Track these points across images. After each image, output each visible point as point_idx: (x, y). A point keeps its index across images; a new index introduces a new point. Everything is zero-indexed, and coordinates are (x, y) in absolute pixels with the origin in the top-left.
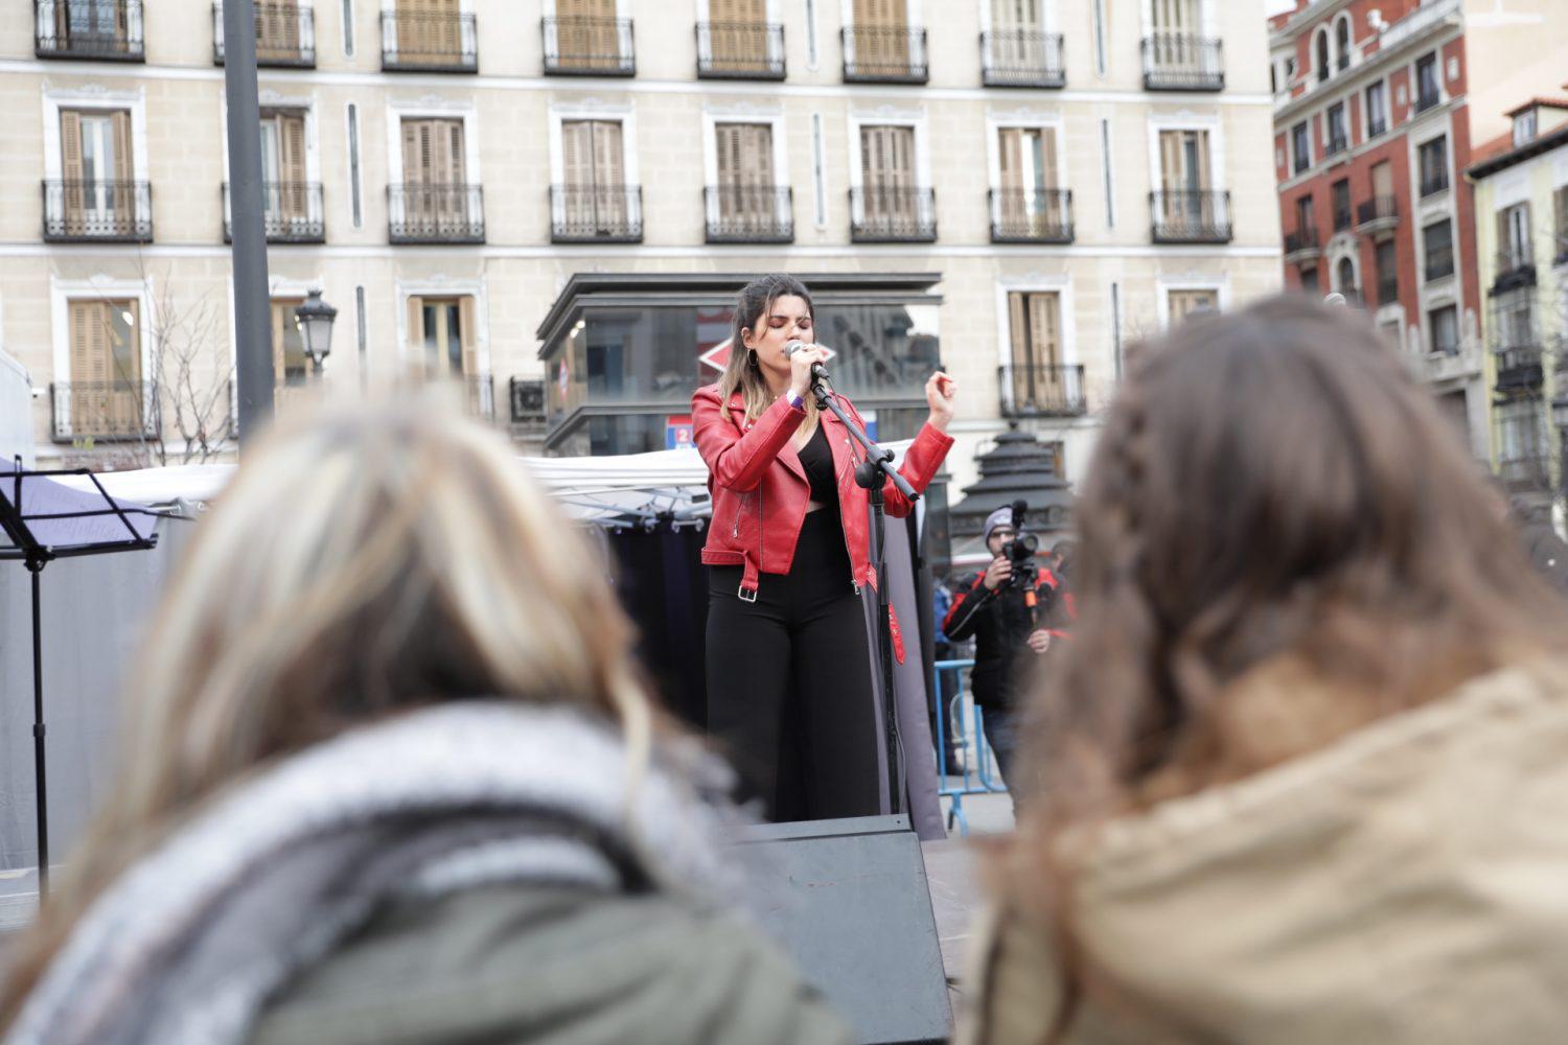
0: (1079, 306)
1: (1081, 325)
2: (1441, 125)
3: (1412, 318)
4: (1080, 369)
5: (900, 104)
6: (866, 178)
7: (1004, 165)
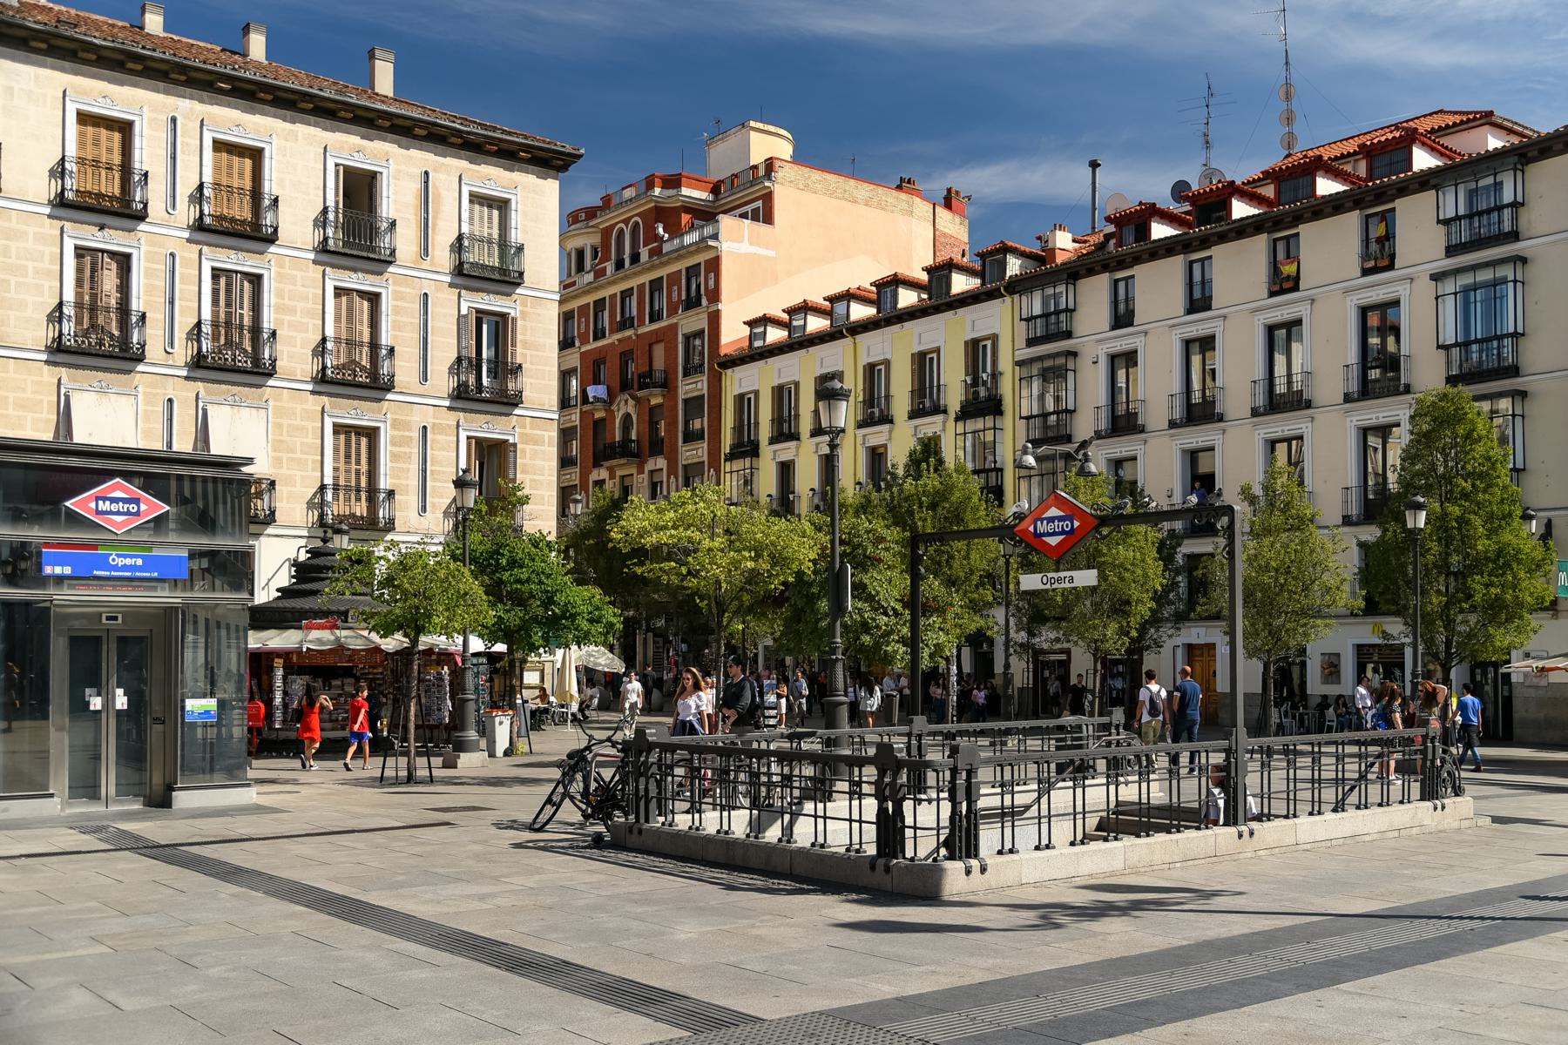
3: (672, 470)
4: (391, 493)
6: (215, 314)
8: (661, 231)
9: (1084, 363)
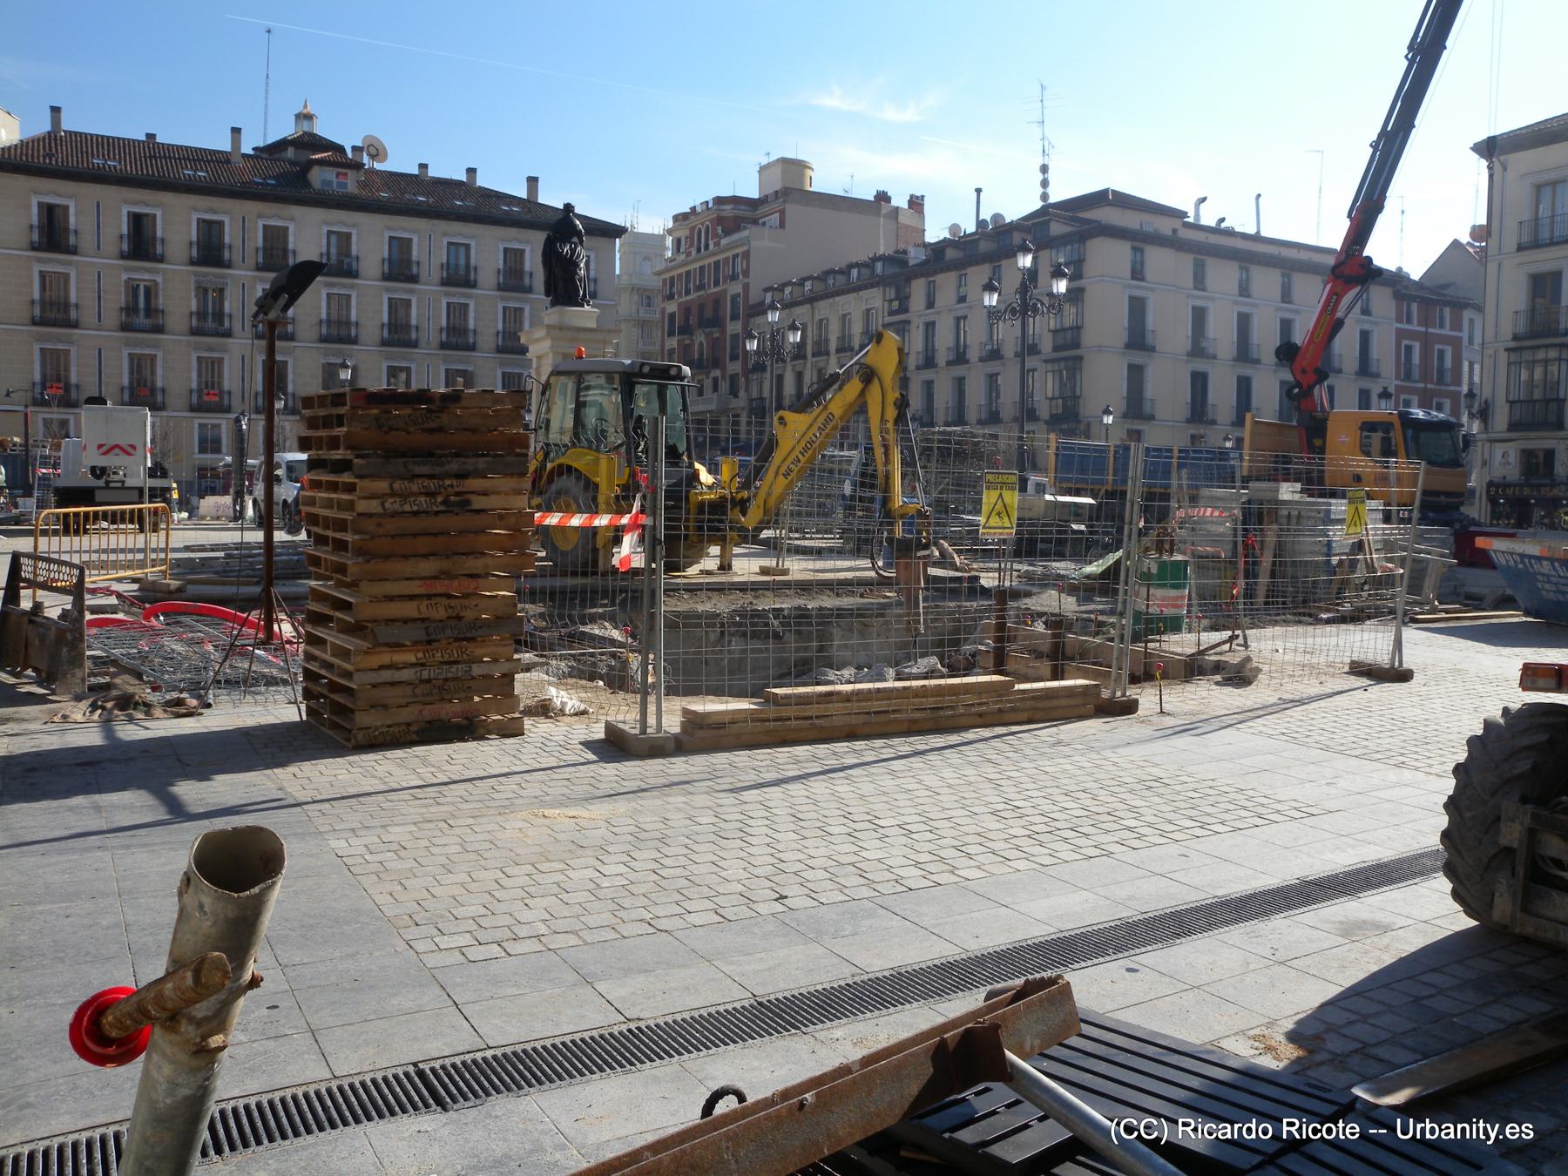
3: (723, 377)
9: (913, 327)
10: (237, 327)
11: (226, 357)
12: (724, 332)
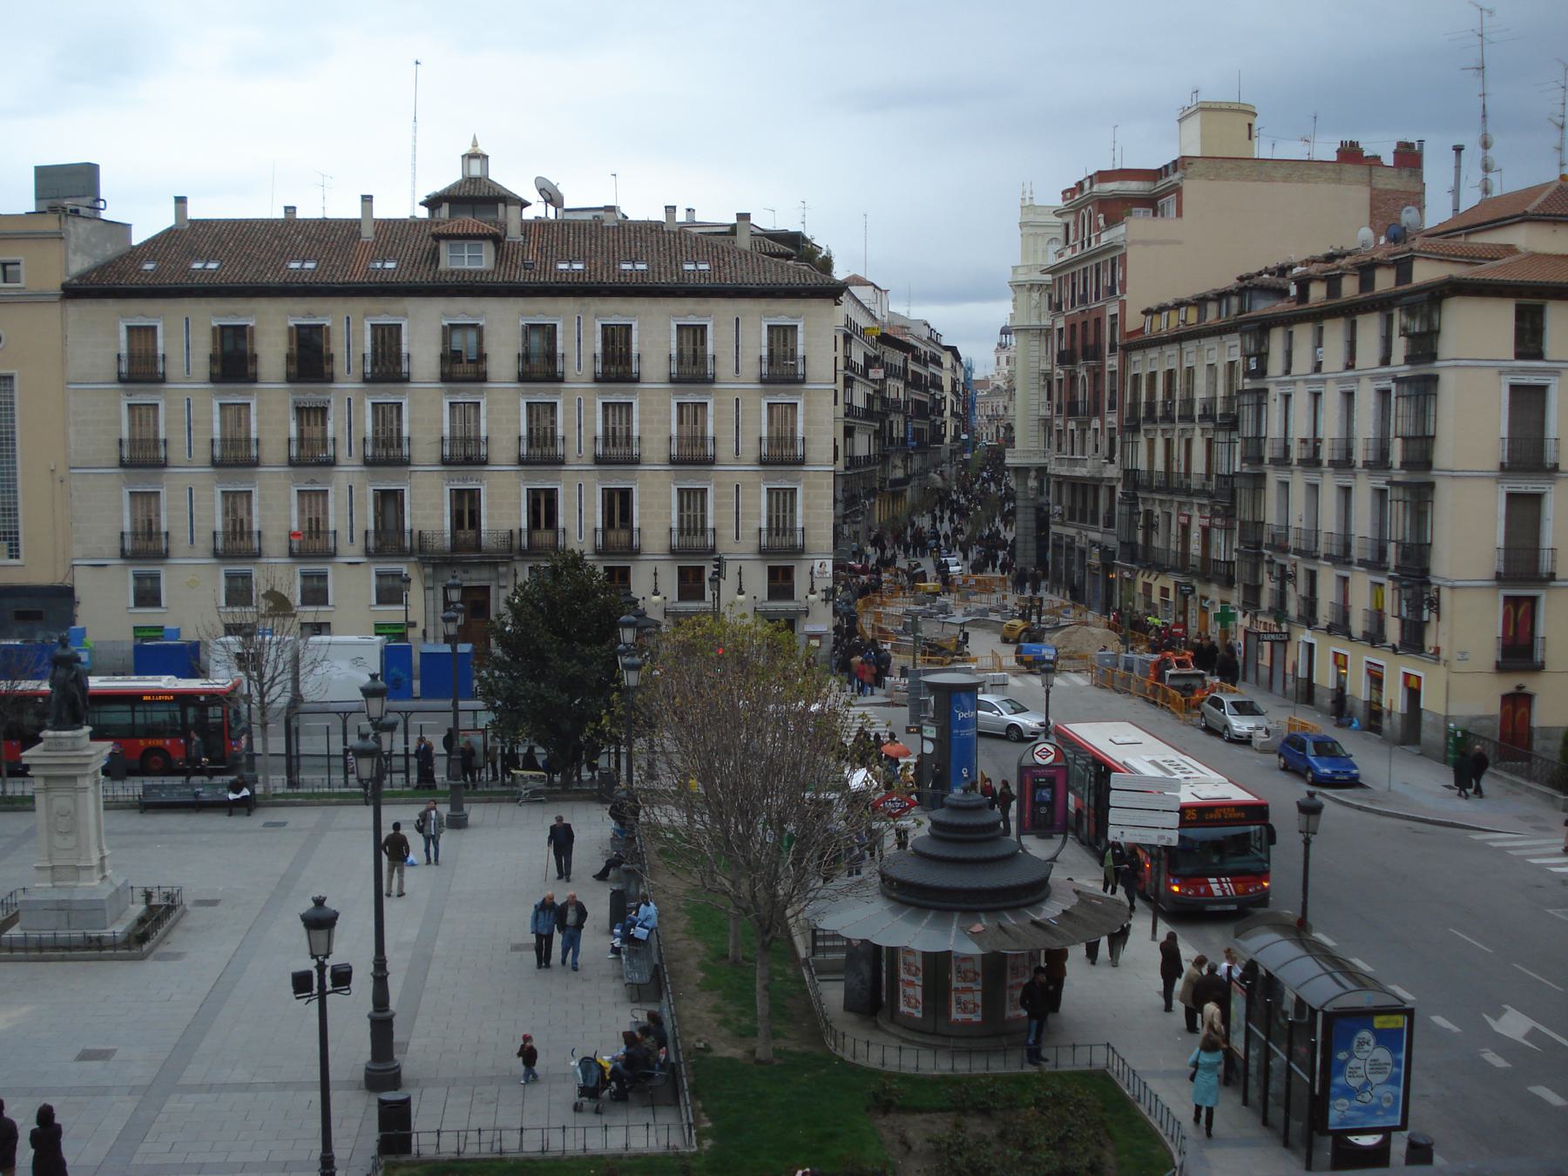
0: (716, 497)
1: (717, 506)
2: (1113, 309)
5: (625, 392)
6: (606, 430)
7: (680, 422)
8: (1101, 222)
10: (343, 454)
11: (331, 491)
12: (1102, 367)
